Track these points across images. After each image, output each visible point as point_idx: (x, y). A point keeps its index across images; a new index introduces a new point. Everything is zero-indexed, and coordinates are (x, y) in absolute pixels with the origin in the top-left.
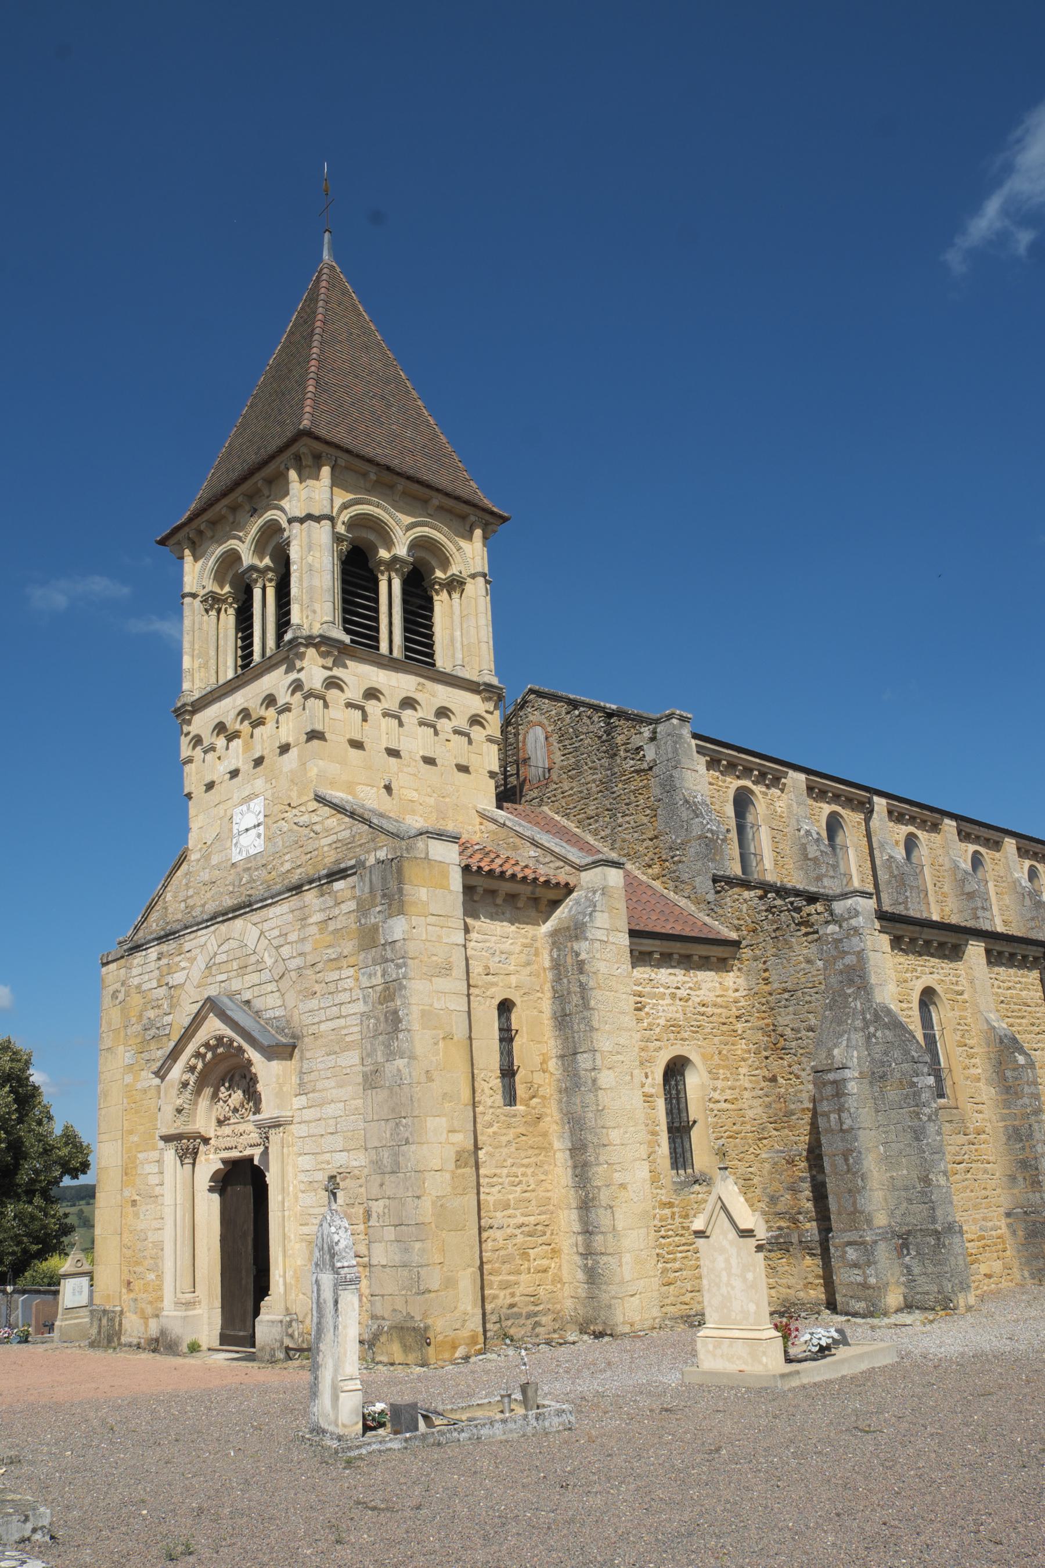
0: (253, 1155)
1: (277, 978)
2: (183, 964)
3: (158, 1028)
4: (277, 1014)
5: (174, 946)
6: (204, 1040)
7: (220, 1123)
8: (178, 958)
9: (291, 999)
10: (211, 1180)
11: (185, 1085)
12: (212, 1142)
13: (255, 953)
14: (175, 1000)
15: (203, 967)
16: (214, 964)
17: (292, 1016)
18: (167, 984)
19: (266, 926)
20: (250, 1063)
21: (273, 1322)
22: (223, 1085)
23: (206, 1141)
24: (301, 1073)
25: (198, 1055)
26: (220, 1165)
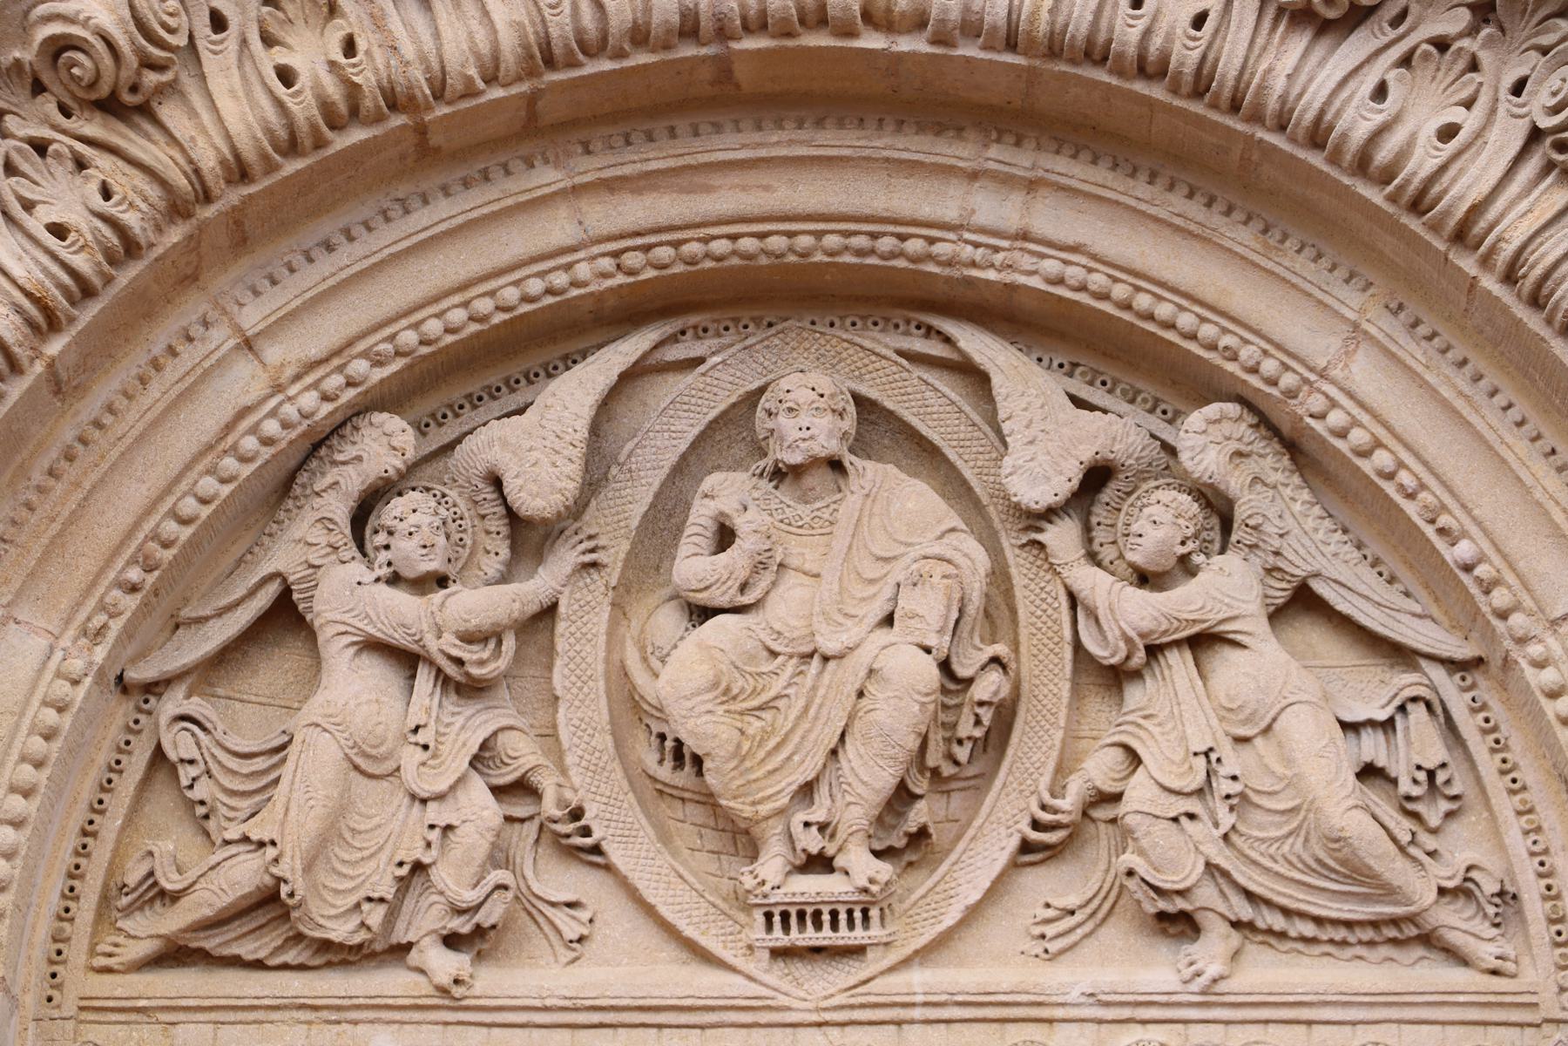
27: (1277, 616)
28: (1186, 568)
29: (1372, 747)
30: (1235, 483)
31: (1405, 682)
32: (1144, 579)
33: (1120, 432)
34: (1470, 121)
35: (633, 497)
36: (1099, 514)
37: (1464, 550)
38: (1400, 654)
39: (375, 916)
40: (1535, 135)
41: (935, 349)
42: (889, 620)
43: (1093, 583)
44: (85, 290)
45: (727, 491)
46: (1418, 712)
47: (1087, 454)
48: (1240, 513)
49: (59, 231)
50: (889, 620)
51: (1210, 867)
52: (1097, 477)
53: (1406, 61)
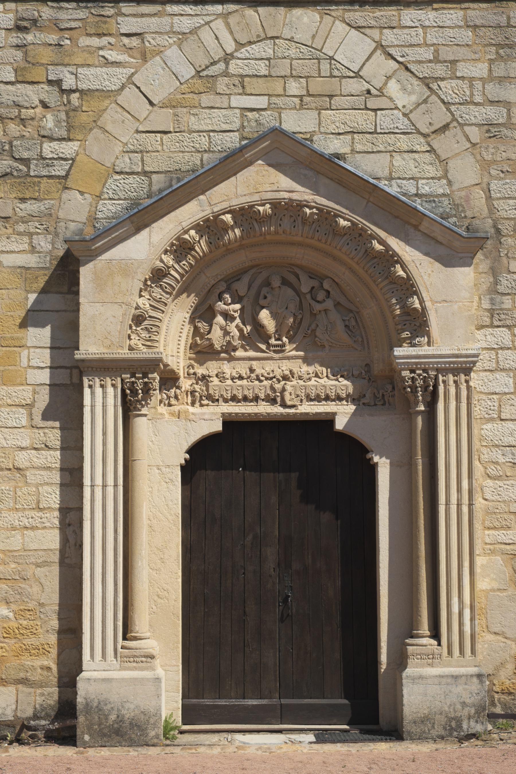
0: (334, 414)
1: (425, 130)
2: (112, 55)
3: (26, 162)
4: (425, 190)
5: (82, 14)
6: (236, 202)
7: (203, 352)
8: (95, 42)
9: (465, 172)
10: (188, 452)
11: (158, 275)
12: (186, 384)
13: (357, 75)
14: (84, 118)
15: (187, 72)
16: (226, 74)
17: (467, 199)
18: (58, 83)
19: (389, 37)
20: (391, 258)
21: (456, 677)
22: (228, 290)
23: (170, 380)
24: (494, 290)
25: (210, 227)
26: (218, 427)
27: (335, 306)
28: (324, 300)
29: (347, 323)
30: (330, 290)
31: (351, 315)
32: (318, 302)
33: (315, 283)
34: (359, 248)
35: (253, 291)
36: (313, 292)
37: (358, 300)
38: (351, 311)
39: (224, 347)
40: (366, 251)
41: (291, 270)
42: (287, 308)
43: (313, 303)
44: (187, 272)
45: (264, 290)
46: (352, 319)
47: (312, 286)
48: (331, 293)
49: (184, 265)
50: (287, 308)
51: (327, 340)
52: (313, 288)
53: (351, 240)
